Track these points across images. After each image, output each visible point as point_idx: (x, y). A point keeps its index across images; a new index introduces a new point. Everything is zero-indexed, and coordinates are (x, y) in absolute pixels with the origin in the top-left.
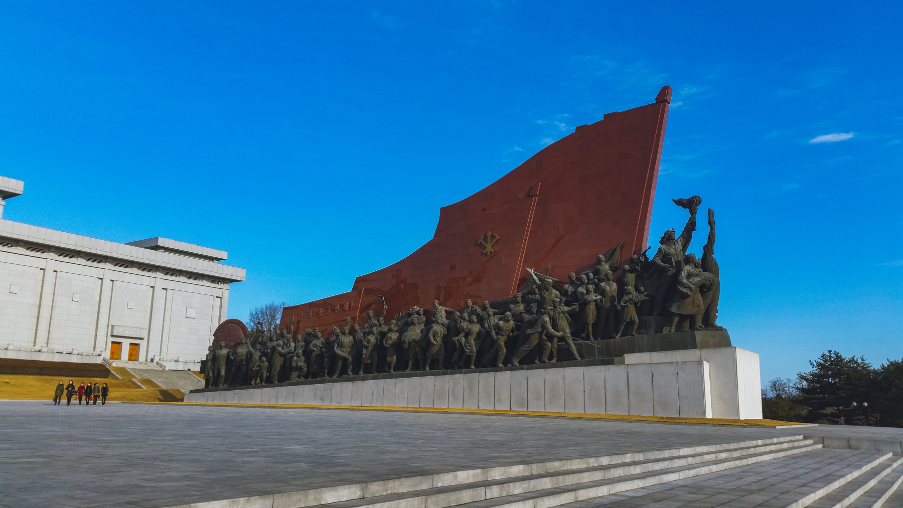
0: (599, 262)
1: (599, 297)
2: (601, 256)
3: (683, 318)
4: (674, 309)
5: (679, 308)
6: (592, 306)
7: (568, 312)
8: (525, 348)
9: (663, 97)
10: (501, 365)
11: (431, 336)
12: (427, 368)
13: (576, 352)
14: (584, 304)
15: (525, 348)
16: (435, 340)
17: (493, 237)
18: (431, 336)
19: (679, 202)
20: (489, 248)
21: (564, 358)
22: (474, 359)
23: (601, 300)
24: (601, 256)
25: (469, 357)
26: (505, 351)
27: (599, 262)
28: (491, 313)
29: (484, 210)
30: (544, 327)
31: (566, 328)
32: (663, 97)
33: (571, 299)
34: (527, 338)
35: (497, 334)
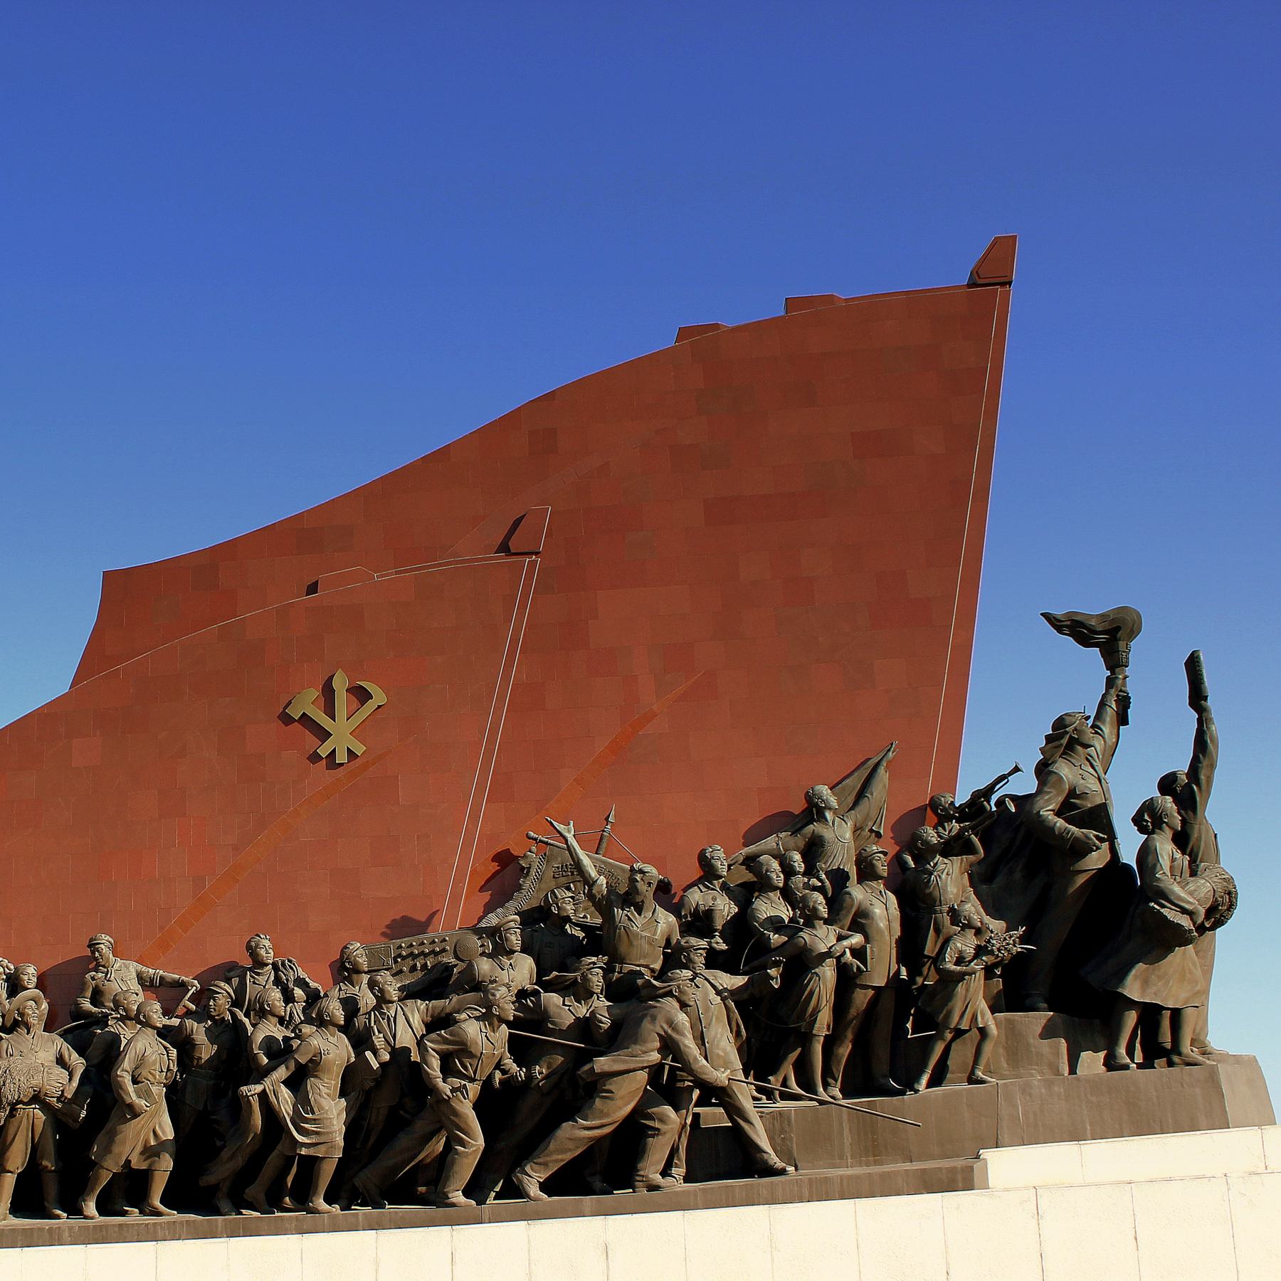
0: (814, 811)
1: (857, 939)
2: (824, 790)
3: (1150, 1014)
4: (1133, 989)
5: (1146, 983)
6: (828, 972)
7: (734, 993)
8: (575, 1135)
9: (991, 278)
10: (458, 1197)
11: (127, 1080)
12: (91, 1207)
13: (764, 1143)
14: (801, 963)
15: (575, 1135)
16: (147, 1094)
17: (361, 695)
18: (127, 1080)
19: (1075, 629)
20: (343, 734)
21: (727, 1162)
22: (327, 1172)
23: (859, 953)
24: (824, 790)
25: (310, 1165)
26: (480, 1142)
27: (814, 811)
28: (393, 991)
29: (313, 588)
30: (669, 1046)
31: (721, 1059)
32: (991, 278)
33: (742, 945)
34: (594, 1087)
35: (447, 1070)
